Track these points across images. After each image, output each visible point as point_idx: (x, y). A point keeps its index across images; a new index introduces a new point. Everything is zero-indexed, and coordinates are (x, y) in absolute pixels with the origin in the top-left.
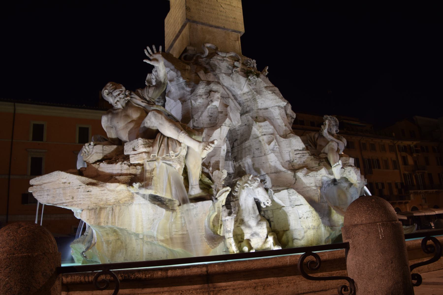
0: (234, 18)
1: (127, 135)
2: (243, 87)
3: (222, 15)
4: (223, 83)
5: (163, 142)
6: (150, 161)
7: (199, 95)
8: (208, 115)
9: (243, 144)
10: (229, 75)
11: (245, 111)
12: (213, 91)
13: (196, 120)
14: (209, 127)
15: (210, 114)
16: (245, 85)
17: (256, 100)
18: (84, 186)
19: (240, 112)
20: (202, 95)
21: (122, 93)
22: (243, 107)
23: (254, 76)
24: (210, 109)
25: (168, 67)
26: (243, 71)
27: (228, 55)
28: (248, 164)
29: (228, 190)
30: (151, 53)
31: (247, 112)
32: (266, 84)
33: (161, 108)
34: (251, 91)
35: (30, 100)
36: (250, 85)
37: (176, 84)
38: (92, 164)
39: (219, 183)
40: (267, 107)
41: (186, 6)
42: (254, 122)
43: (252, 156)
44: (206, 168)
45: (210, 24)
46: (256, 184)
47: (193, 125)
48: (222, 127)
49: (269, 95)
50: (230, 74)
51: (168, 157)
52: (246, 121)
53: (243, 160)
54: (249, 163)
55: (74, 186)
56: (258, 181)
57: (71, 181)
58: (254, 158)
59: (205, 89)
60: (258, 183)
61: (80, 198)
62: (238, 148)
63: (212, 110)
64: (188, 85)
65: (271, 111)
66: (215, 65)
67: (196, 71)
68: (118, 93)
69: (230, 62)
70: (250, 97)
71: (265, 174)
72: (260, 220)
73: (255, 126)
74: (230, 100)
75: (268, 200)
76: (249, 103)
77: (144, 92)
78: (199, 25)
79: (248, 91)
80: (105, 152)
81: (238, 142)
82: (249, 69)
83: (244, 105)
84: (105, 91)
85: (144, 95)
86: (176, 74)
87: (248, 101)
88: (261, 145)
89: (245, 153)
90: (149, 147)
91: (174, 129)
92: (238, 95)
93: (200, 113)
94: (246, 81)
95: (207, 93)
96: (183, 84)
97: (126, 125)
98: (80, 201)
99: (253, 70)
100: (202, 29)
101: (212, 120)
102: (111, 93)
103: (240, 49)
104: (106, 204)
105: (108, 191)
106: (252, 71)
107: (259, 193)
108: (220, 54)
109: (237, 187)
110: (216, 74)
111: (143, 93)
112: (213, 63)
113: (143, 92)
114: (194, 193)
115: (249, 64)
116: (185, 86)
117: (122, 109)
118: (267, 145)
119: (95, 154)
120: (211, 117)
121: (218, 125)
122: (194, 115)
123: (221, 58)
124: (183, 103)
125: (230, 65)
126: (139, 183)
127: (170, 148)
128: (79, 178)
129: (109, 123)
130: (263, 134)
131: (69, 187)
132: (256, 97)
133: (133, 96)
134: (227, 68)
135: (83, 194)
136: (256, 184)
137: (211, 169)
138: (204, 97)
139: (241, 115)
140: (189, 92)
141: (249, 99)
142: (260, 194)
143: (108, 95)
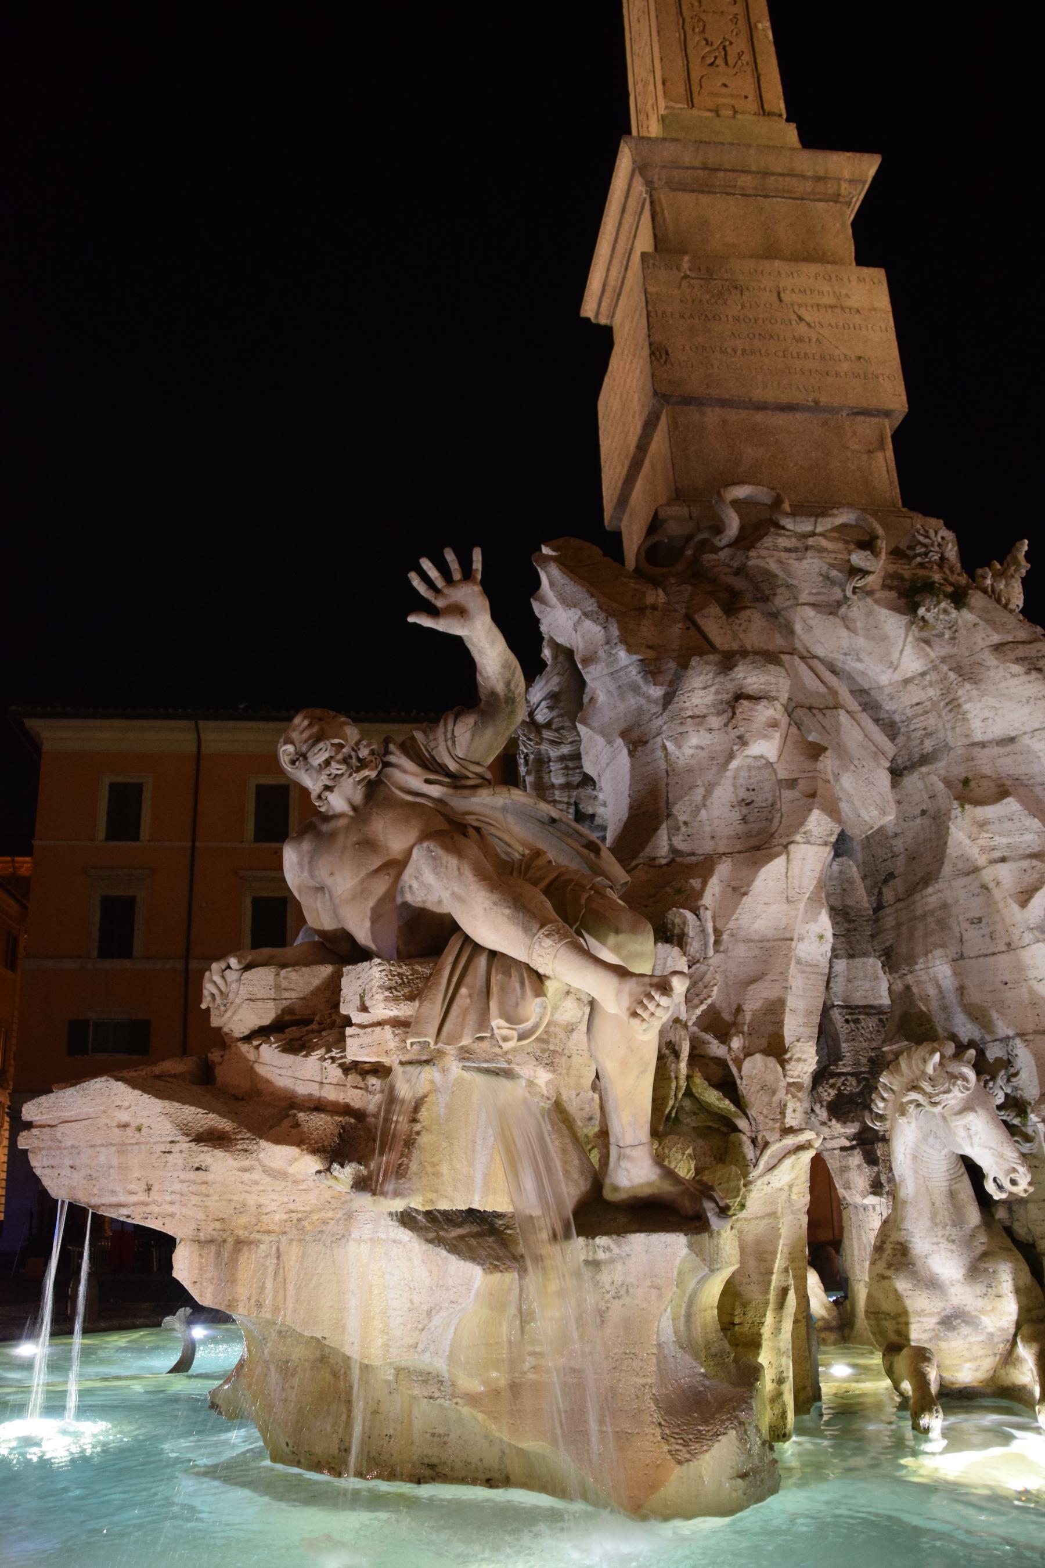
0: (859, 358)
1: (368, 924)
2: (897, 654)
3: (806, 354)
4: (808, 644)
5: (468, 979)
6: (410, 1063)
7: (690, 717)
8: (737, 796)
9: (917, 897)
10: (832, 609)
11: (916, 756)
12: (749, 697)
13: (685, 823)
14: (739, 852)
15: (742, 794)
16: (904, 645)
17: (959, 706)
18: (184, 1144)
19: (888, 765)
20: (704, 716)
21: (340, 757)
22: (909, 739)
23: (943, 605)
24: (744, 774)
25: (575, 606)
26: (896, 583)
27: (824, 525)
28: (939, 986)
29: (809, 1141)
30: (440, 583)
31: (925, 759)
32: (998, 633)
33: (514, 797)
34: (935, 668)
35: (242, 706)
36: (927, 642)
37: (605, 672)
38: (239, 1044)
39: (765, 1112)
40: (1013, 734)
41: (650, 344)
42: (955, 804)
43: (953, 950)
44: (716, 1042)
45: (755, 399)
46: (956, 1096)
47: (671, 846)
48: (792, 848)
49: (1014, 681)
50: (839, 604)
51: (485, 1045)
52: (926, 797)
53: (917, 967)
54: (941, 982)
55: (155, 1143)
56: (965, 1079)
57: (145, 1122)
58: (960, 962)
59: (713, 689)
60: (968, 1092)
61: (172, 1192)
62: (897, 911)
63: (750, 777)
64: (650, 672)
65: (1029, 751)
66: (769, 576)
67: (688, 608)
68: (326, 755)
69: (833, 555)
70: (931, 692)
71: (1011, 1033)
72: (984, 1256)
73: (959, 819)
74: (843, 717)
75: (1014, 1170)
76: (931, 721)
77: (435, 739)
78: (709, 411)
79: (920, 671)
80: (286, 995)
81: (899, 884)
82: (921, 572)
83: (912, 727)
84: (284, 748)
85: (434, 753)
86: (603, 631)
87: (927, 712)
88: (990, 903)
89: (926, 935)
90: (411, 998)
91: (508, 918)
92: (880, 688)
93: (701, 791)
94: (908, 630)
95: (724, 706)
96: (634, 673)
97: (362, 882)
98: (172, 1203)
99: (937, 577)
100: (725, 422)
101: (750, 818)
102: (304, 756)
103: (891, 483)
104: (257, 1228)
105: (264, 1176)
106: (933, 583)
107: (970, 1137)
108: (788, 523)
109: (883, 1099)
110: (778, 612)
111: (432, 744)
112: (758, 566)
113: (431, 738)
114: (630, 1180)
115: (920, 550)
116: (639, 679)
117: (352, 817)
118: (1015, 907)
119: (245, 1006)
120: (748, 804)
121: (775, 842)
122: (675, 803)
123: (793, 539)
124: (635, 749)
125: (832, 566)
126: (354, 1165)
127: (494, 1005)
128: (172, 1111)
129: (306, 874)
130: (997, 854)
131: (137, 1144)
132: (960, 693)
133: (392, 759)
134: (821, 578)
135: (182, 1177)
136: (954, 1097)
137: (736, 1043)
138: (715, 722)
139: (897, 773)
140: (656, 702)
141: (928, 703)
142: (976, 1140)
143: (293, 762)
